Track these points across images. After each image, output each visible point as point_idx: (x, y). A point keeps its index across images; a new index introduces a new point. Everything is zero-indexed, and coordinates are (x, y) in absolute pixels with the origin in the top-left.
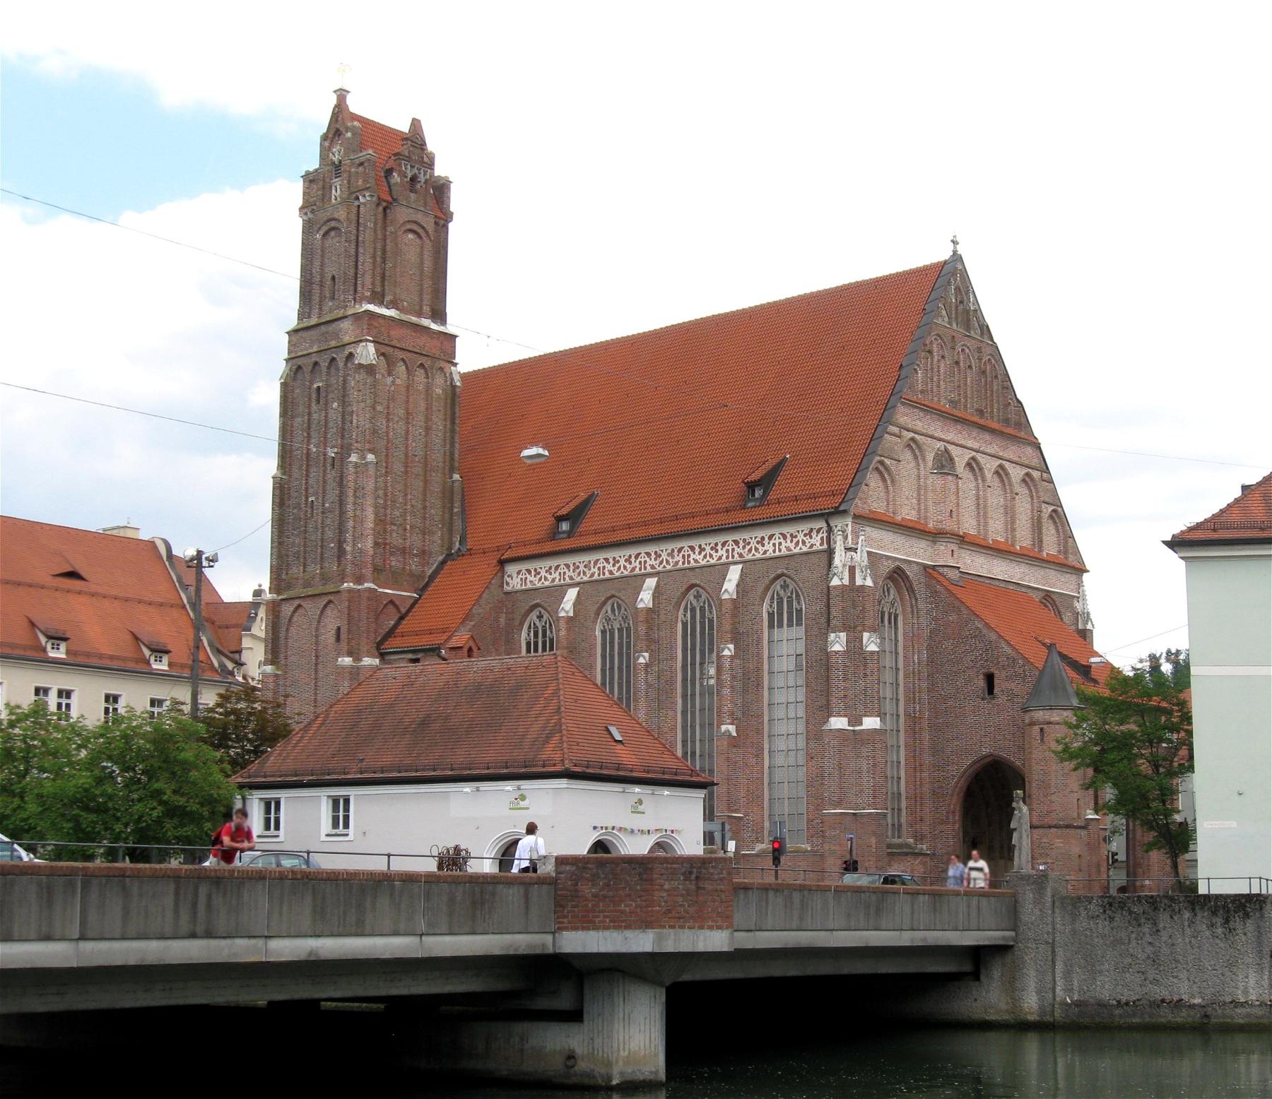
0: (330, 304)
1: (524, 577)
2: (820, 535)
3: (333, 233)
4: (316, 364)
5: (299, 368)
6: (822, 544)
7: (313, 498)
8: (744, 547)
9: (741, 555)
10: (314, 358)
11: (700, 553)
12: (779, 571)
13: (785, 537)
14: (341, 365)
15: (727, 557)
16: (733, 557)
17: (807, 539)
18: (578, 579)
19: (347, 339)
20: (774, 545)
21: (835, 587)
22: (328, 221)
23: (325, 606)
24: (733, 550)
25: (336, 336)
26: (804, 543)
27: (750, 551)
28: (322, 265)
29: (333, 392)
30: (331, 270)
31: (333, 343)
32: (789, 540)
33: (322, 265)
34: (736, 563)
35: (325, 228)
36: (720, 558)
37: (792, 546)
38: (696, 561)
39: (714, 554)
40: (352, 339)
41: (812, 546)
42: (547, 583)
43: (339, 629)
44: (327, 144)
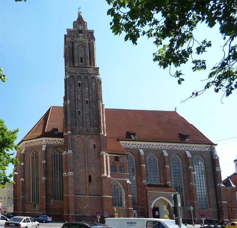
0: (81, 63)
1: (124, 145)
2: (208, 148)
3: (80, 46)
4: (79, 76)
5: (72, 76)
6: (208, 150)
7: (80, 110)
8: (189, 148)
9: (188, 149)
10: (78, 75)
11: (177, 147)
12: (198, 154)
13: (199, 147)
14: (90, 79)
15: (184, 149)
16: (186, 149)
17: (205, 149)
18: (142, 148)
19: (91, 73)
20: (196, 148)
21: (217, 159)
22: (80, 42)
23: (90, 138)
24: (186, 148)
25: (87, 71)
26: (204, 149)
27: (190, 149)
28: (78, 53)
29: (86, 85)
30: (81, 55)
31: (85, 73)
32: (200, 148)
33: (78, 53)
34: (187, 150)
35: (78, 44)
36: (182, 149)
37: (201, 149)
38: (176, 148)
39: (181, 148)
40: (93, 73)
41: (206, 150)
42: (132, 147)
43: (94, 145)
44: (76, 24)
